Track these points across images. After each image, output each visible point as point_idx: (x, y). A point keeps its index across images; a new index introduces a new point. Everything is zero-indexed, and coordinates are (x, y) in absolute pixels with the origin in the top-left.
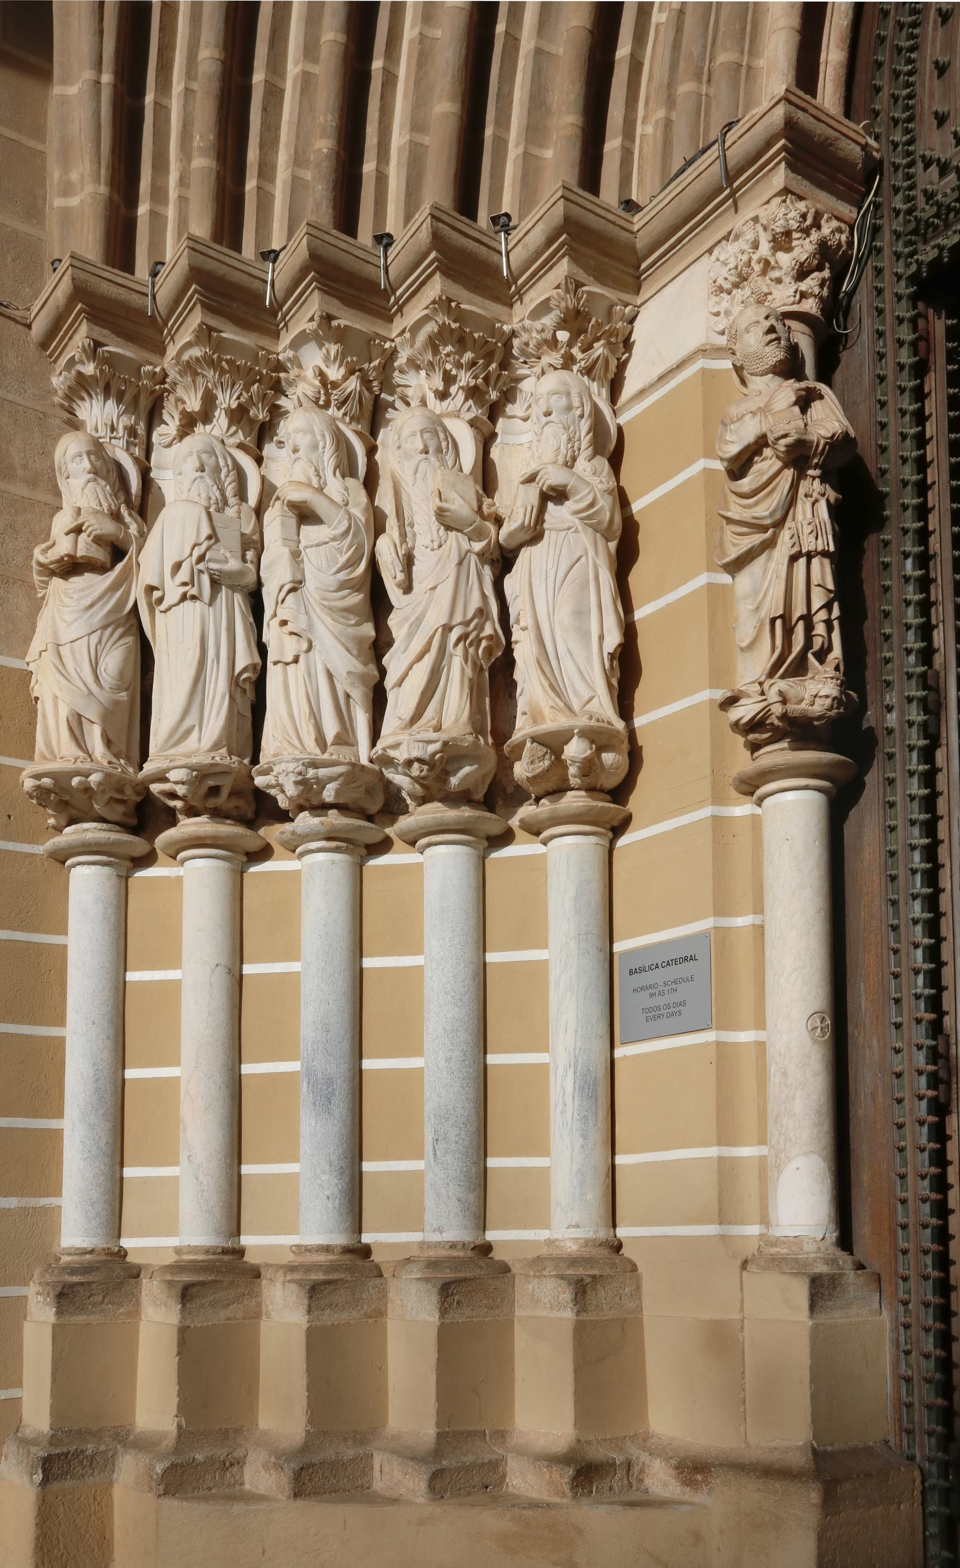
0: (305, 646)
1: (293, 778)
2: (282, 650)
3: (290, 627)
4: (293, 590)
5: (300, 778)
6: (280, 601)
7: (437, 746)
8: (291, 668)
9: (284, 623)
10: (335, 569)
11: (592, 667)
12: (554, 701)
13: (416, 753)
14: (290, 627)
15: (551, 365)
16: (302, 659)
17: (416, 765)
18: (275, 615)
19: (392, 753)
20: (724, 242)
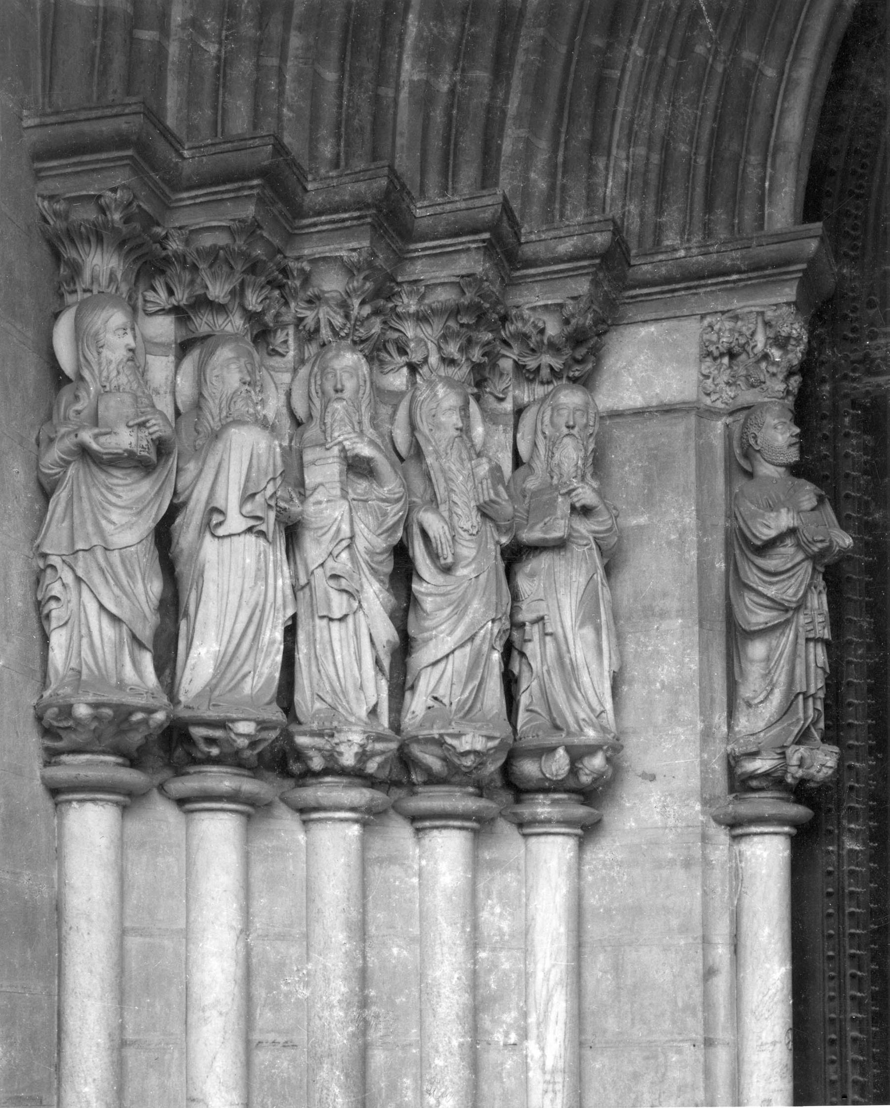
0: (355, 605)
1: (356, 749)
2: (329, 607)
3: (344, 583)
4: (349, 546)
5: (361, 750)
6: (335, 553)
7: (496, 742)
8: (335, 626)
9: (335, 577)
10: (380, 531)
11: (603, 683)
12: (589, 718)
13: (479, 747)
14: (344, 583)
15: (552, 369)
16: (350, 620)
17: (472, 757)
18: (322, 565)
19: (449, 740)
20: (720, 314)
